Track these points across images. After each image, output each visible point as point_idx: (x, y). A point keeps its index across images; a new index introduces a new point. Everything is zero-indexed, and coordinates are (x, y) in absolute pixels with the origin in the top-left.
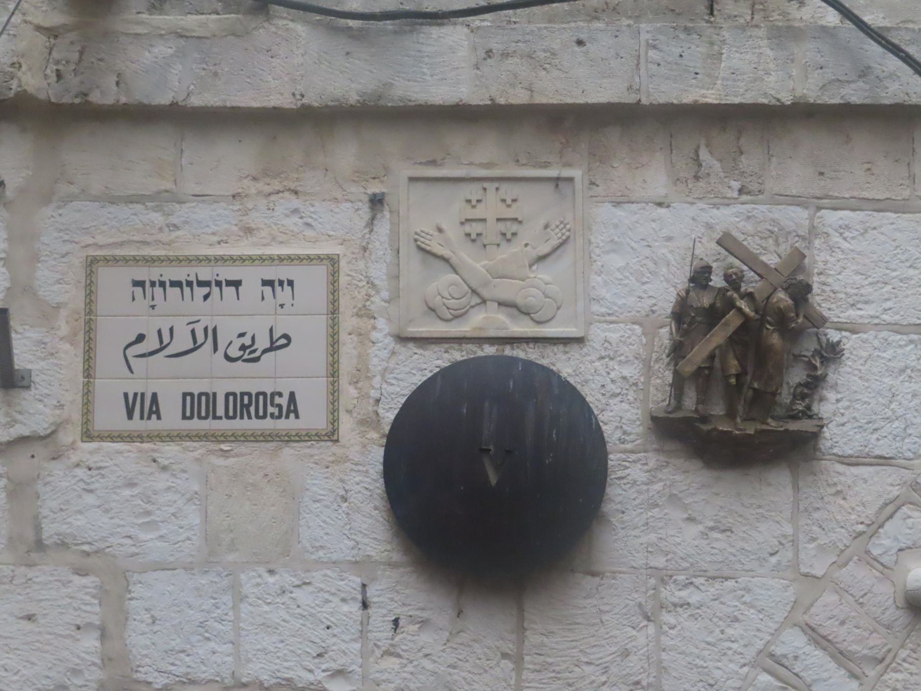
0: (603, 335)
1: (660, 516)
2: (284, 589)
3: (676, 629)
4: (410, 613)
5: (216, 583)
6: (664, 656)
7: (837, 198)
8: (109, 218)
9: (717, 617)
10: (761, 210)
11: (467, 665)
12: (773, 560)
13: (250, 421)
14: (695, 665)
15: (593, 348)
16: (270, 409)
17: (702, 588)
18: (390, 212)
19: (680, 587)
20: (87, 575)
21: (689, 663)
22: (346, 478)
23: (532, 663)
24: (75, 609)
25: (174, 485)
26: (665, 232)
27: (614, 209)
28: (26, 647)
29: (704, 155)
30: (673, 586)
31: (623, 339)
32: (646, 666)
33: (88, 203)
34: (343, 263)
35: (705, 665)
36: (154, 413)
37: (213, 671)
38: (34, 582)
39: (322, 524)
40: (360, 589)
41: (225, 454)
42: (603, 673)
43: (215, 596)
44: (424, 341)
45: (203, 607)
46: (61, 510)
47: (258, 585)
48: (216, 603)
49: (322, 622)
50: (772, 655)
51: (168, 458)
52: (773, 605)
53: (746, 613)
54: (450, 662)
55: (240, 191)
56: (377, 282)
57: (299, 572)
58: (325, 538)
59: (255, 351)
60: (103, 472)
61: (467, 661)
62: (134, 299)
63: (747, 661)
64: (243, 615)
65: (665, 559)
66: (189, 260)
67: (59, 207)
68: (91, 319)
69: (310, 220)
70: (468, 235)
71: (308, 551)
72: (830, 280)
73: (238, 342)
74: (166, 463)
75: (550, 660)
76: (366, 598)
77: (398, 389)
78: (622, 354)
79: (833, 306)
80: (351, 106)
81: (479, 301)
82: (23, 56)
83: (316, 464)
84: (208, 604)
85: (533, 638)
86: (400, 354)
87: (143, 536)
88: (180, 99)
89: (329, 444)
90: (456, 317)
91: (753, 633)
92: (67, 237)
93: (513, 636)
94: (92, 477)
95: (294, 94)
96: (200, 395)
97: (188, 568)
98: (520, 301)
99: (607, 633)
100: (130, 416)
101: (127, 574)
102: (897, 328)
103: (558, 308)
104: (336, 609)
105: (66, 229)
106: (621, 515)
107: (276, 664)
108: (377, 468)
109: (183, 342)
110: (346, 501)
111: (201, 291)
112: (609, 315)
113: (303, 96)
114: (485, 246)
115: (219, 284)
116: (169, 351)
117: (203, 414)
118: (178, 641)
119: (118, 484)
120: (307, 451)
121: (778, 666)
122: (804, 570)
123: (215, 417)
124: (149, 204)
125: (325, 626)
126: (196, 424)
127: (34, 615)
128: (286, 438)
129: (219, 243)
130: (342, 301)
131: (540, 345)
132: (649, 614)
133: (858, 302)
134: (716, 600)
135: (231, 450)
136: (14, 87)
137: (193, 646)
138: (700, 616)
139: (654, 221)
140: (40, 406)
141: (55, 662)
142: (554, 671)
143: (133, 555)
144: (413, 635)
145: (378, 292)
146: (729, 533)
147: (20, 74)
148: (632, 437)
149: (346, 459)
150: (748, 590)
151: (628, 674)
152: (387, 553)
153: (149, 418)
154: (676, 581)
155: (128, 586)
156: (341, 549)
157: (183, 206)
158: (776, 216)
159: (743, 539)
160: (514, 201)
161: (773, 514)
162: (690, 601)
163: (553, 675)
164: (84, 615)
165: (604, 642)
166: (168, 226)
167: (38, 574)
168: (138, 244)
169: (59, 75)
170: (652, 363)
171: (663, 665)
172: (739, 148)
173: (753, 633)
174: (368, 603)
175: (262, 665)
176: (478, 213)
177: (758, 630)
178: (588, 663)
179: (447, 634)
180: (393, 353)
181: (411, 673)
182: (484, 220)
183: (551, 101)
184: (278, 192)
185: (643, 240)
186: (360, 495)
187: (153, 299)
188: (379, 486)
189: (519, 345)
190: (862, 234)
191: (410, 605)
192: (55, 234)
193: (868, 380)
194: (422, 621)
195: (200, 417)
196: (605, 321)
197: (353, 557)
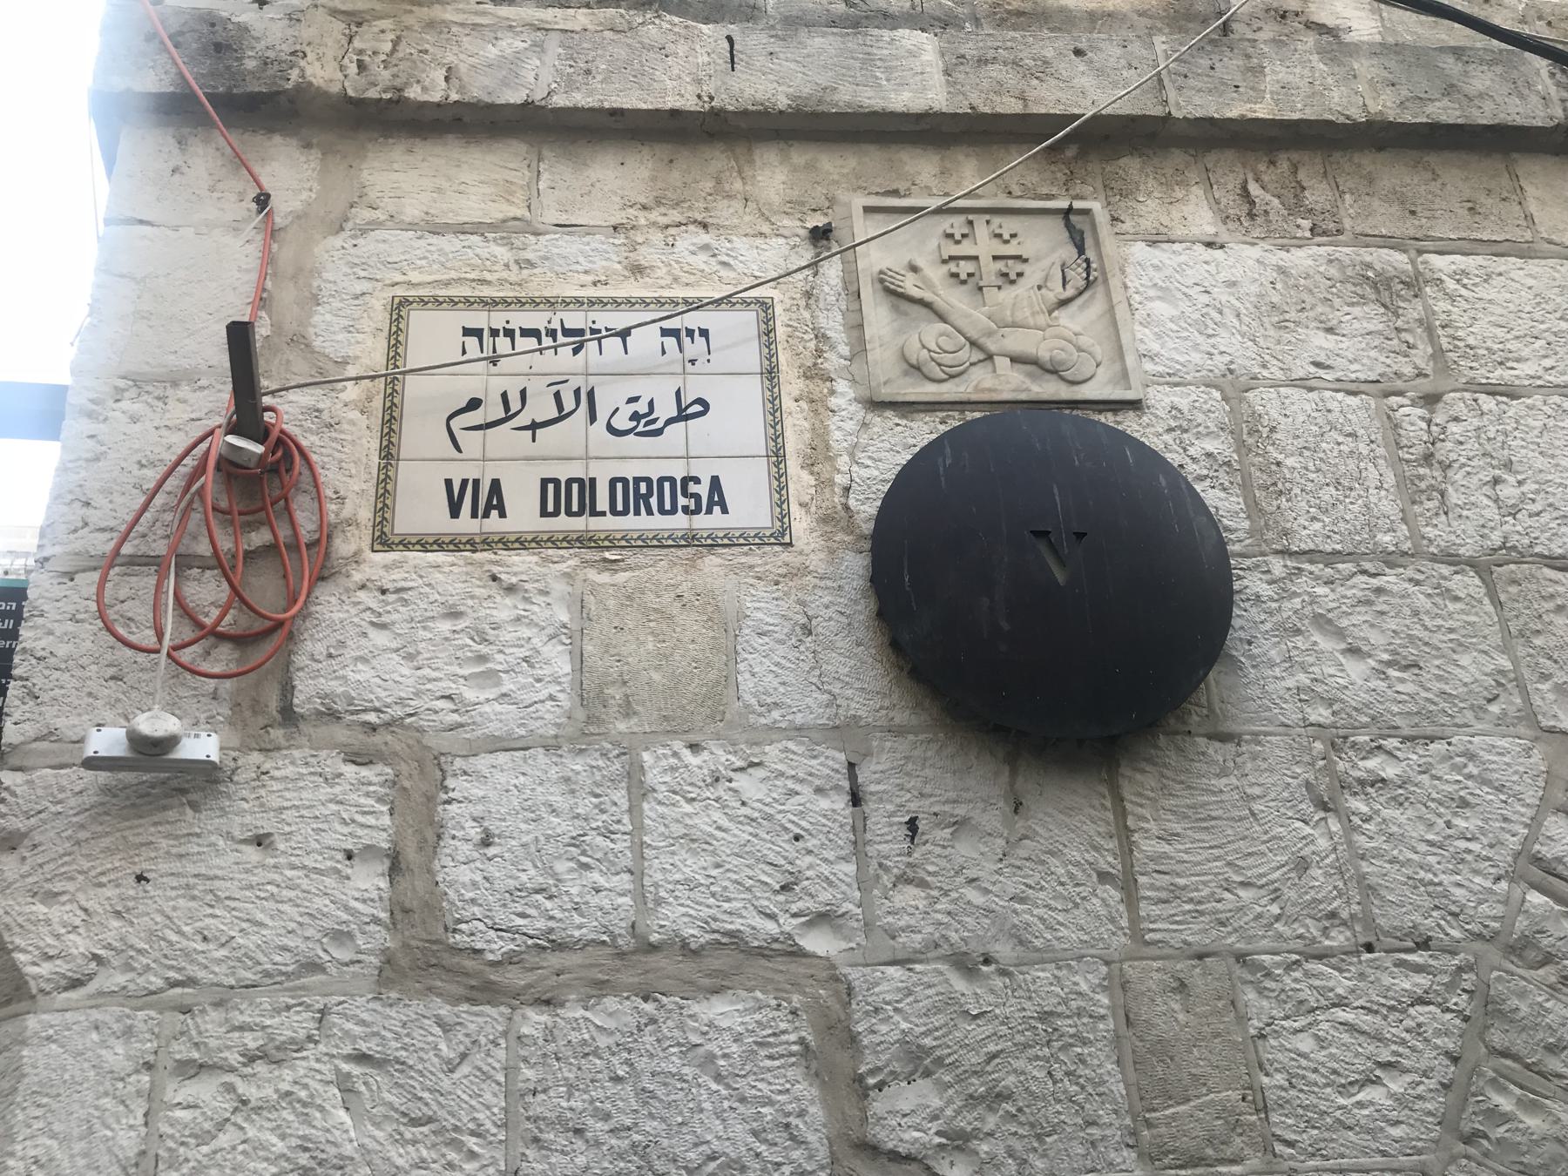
0: (1167, 400)
1: (1307, 646)
2: (717, 774)
3: (1372, 823)
4: (936, 809)
5: (599, 768)
6: (1365, 867)
7: (1441, 239)
8: (428, 251)
9: (1433, 800)
10: (1345, 252)
11: (1042, 895)
12: (1494, 709)
14: (1421, 881)
15: (1157, 417)
16: (682, 501)
17: (1398, 753)
19: (1364, 753)
20: (371, 762)
21: (1409, 878)
23: (1152, 887)
24: (344, 822)
25: (526, 614)
26: (1223, 276)
28: (248, 893)
29: (1254, 189)
30: (1351, 753)
31: (1197, 404)
32: (1340, 884)
34: (778, 310)
35: (1436, 880)
36: (495, 507)
37: (595, 924)
38: (272, 778)
39: (774, 669)
40: (845, 771)
42: (1273, 900)
44: (906, 408)
45: (579, 811)
46: (330, 656)
47: (673, 769)
48: (601, 803)
49: (786, 829)
50: (1537, 860)
51: (515, 574)
52: (1515, 778)
53: (1478, 792)
54: (1012, 891)
55: (625, 221)
56: (829, 334)
57: (743, 746)
58: (782, 689)
59: (654, 421)
60: (405, 596)
61: (1042, 889)
63: (1502, 872)
64: (647, 821)
65: (1330, 711)
66: (551, 303)
67: (354, 237)
69: (725, 259)
70: (955, 275)
71: (754, 712)
72: (1460, 333)
74: (514, 580)
75: (1181, 881)
77: (876, 473)
79: (1474, 364)
80: (781, 112)
81: (981, 356)
82: (309, 44)
83: (759, 578)
84: (585, 805)
85: (1147, 846)
86: (874, 425)
87: (470, 694)
88: (538, 96)
89: (777, 548)
90: (952, 377)
91: (1498, 825)
92: (363, 274)
93: (1112, 844)
94: (388, 604)
95: (699, 97)
96: (570, 482)
97: (551, 746)
98: (1044, 354)
99: (1266, 832)
100: (455, 511)
101: (443, 759)
103: (1097, 366)
104: (808, 805)
107: (709, 906)
108: (855, 583)
113: (712, 98)
114: (980, 289)
116: (516, 422)
117: (575, 508)
118: (532, 872)
119: (431, 614)
120: (743, 559)
121: (1551, 878)
122: (1545, 723)
123: (595, 513)
124: (490, 236)
125: (791, 835)
126: (563, 523)
127: (269, 835)
128: (709, 542)
129: (595, 284)
130: (783, 358)
132: (1326, 799)
133: (1508, 359)
134: (1424, 773)
135: (623, 560)
136: (294, 74)
137: (558, 880)
138: (1407, 799)
141: (300, 919)
142: (1191, 900)
144: (944, 847)
145: (833, 348)
146: (1417, 671)
147: (302, 63)
148: (1241, 535)
149: (803, 571)
150: (1472, 757)
151: (1314, 900)
152: (884, 712)
153: (486, 515)
154: (1354, 744)
155: (444, 779)
157: (541, 238)
158: (1368, 259)
159: (1439, 678)
160: (1013, 236)
161: (1474, 640)
162: (1384, 775)
163: (1187, 907)
164: (360, 832)
165: (1263, 848)
166: (517, 262)
168: (474, 284)
169: (361, 66)
170: (1245, 437)
171: (1367, 882)
172: (1298, 182)
173: (1498, 825)
175: (684, 910)
176: (966, 248)
177: (1506, 819)
178: (1243, 884)
179: (1001, 842)
180: (865, 425)
181: (949, 913)
182: (976, 258)
183: (1052, 111)
184: (679, 225)
188: (864, 610)
190: (1485, 281)
191: (931, 796)
192: (349, 271)
193: (1553, 456)
194: (955, 823)
195: (569, 513)
196: (1168, 383)
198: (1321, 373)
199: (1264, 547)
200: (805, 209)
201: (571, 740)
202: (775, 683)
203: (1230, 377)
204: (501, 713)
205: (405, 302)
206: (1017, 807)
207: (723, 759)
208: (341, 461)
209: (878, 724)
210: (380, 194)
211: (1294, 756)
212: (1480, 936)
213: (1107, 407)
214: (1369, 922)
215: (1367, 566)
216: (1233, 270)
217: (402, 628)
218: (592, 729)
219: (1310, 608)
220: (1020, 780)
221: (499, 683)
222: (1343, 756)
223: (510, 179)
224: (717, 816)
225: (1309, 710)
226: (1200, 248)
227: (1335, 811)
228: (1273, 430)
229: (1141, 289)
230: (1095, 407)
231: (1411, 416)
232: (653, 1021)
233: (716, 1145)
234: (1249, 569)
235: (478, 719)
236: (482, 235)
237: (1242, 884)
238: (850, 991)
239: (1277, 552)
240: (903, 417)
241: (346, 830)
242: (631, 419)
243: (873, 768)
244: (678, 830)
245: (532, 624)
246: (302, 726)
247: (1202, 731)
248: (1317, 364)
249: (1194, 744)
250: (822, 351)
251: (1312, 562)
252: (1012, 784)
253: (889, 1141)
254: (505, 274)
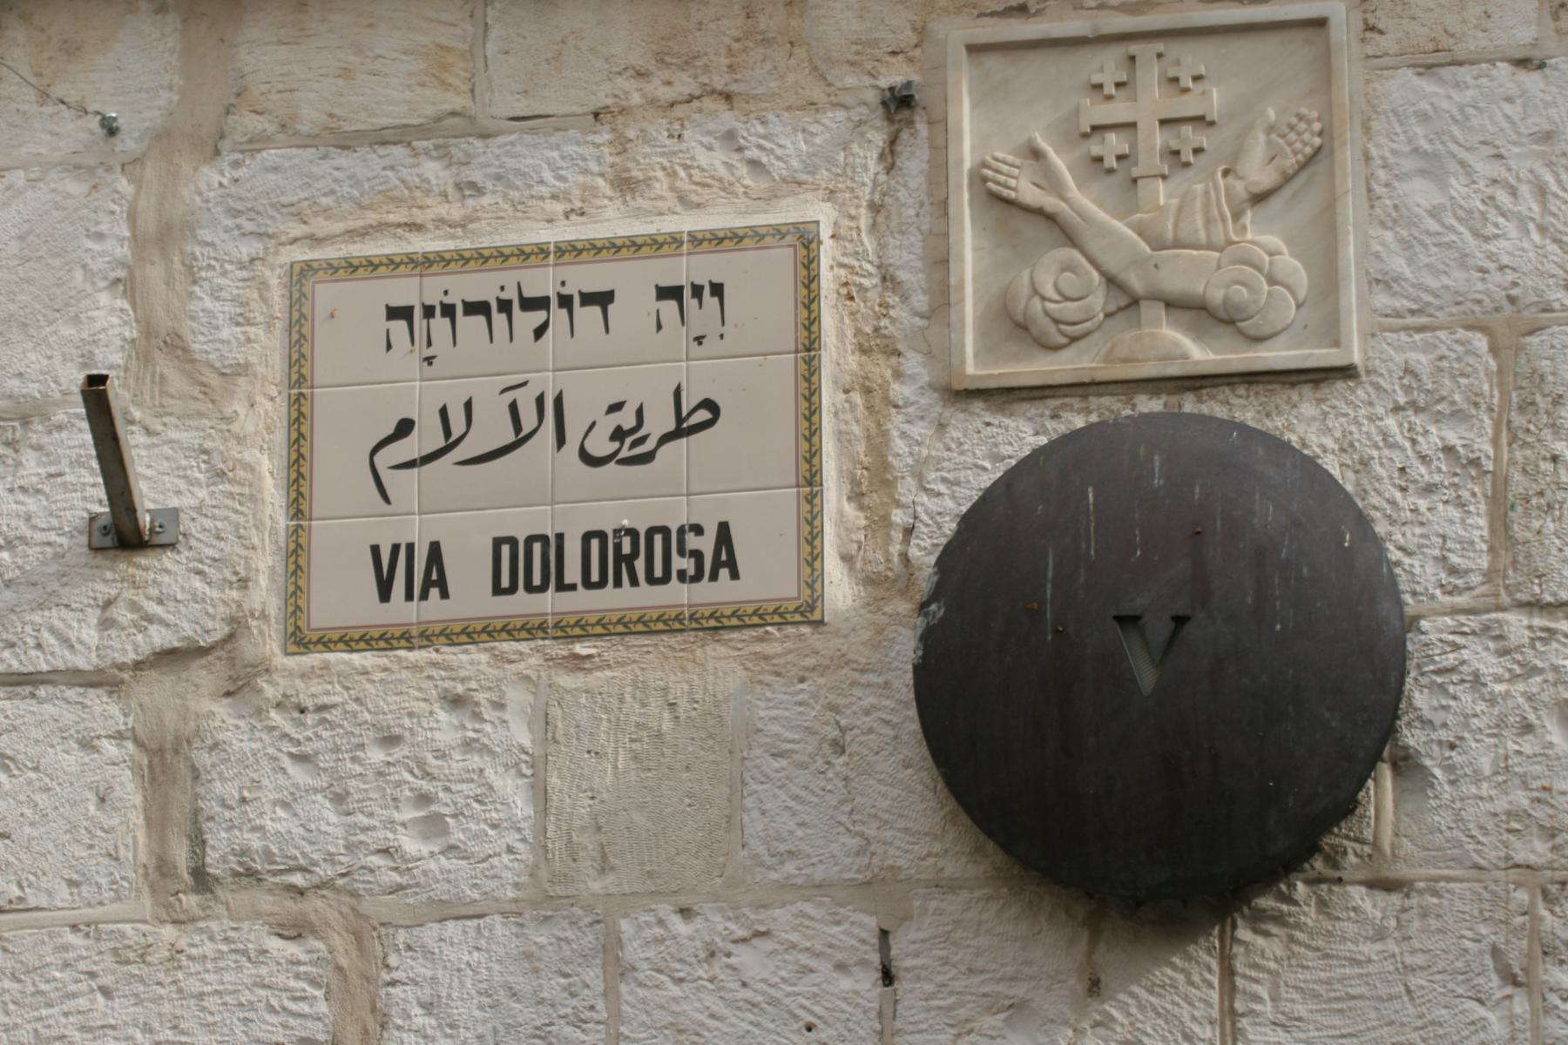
0: (1399, 358)
1: (1537, 750)
2: (713, 948)
4: (986, 989)
5: (567, 940)
8: (336, 181)
13: (635, 589)
15: (1378, 387)
16: (679, 563)
18: (930, 123)
20: (300, 935)
22: (841, 701)
24: (272, 1009)
26: (1538, 122)
27: (1416, 81)
33: (294, 151)
36: (434, 584)
38: (191, 958)
39: (792, 804)
40: (875, 941)
41: (577, 663)
43: (567, 970)
44: (1004, 396)
45: (545, 995)
47: (659, 941)
48: (570, 985)
49: (795, 1016)
55: (609, 101)
56: (902, 275)
58: (800, 833)
59: (642, 440)
60: (328, 716)
62: (389, 347)
64: (625, 1008)
65: (1549, 845)
67: (236, 164)
68: (301, 394)
71: (762, 864)
73: (608, 424)
74: (460, 689)
76: (890, 961)
78: (1443, 399)
81: (1123, 301)
83: (778, 674)
84: (553, 987)
89: (805, 630)
90: (1074, 339)
92: (249, 226)
96: (530, 540)
98: (1216, 296)
99: (1421, 1016)
100: (385, 593)
104: (824, 986)
105: (249, 210)
106: (1447, 754)
109: (492, 430)
110: (843, 752)
111: (527, 321)
112: (1412, 312)
114: (1135, 181)
115: (566, 301)
116: (461, 453)
117: (537, 581)
120: (758, 648)
123: (562, 587)
124: (420, 145)
125: (801, 1024)
126: (521, 603)
128: (712, 623)
131: (1260, 388)
132: (1517, 970)
139: (1509, 100)
140: (197, 583)
143: (398, 889)
145: (905, 298)
149: (843, 660)
152: (931, 860)
153: (424, 596)
156: (833, 856)
164: (292, 1022)
167: (197, 938)
168: (399, 230)
174: (894, 971)
176: (1118, 111)
182: (1132, 125)
184: (690, 99)
185: (1484, 143)
186: (872, 736)
187: (429, 344)
189: (1214, 391)
191: (982, 972)
192: (230, 223)
194: (1011, 1006)
195: (530, 588)
196: (1406, 328)
197: (858, 871)
199: (1505, 599)
200: (878, 53)
201: (534, 904)
202: (792, 824)
203: (1508, 310)
204: (449, 871)
205: (307, 268)
207: (721, 928)
208: (237, 526)
209: (923, 876)
210: (263, 88)
211: (1481, 912)
213: (1303, 378)
216: (1552, 111)
217: (325, 761)
218: (559, 890)
219: (1552, 690)
220: (1102, 947)
221: (445, 831)
222: (1557, 909)
223: (443, 41)
224: (710, 1000)
225: (1518, 845)
226: (1504, 68)
228: (1557, 401)
229: (1392, 160)
230: (1283, 378)
234: (1474, 633)
235: (422, 880)
236: (409, 144)
240: (1001, 410)
241: (274, 1019)
242: (613, 437)
243: (912, 936)
244: (663, 1017)
245: (485, 750)
246: (219, 891)
247: (1359, 876)
249: (1347, 897)
250: (887, 306)
252: (1089, 954)
254: (442, 210)
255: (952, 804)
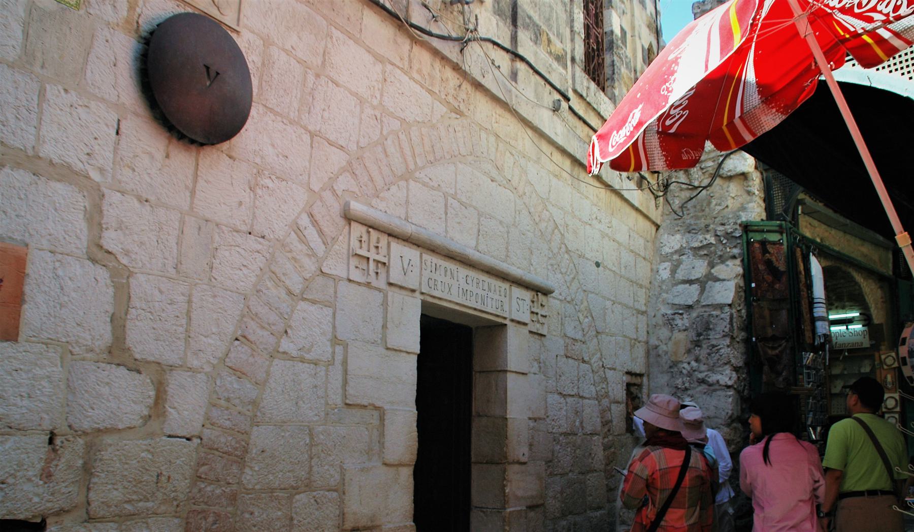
49: (92, 134)
61: (168, 184)
72: (331, 58)
102: (351, 93)
154: (264, 174)
198: (293, 51)
206: (167, 156)
212: (277, 240)
214: (252, 226)
215: (285, 121)
227: (253, 191)
231: (311, 78)
232: (37, 184)
233: (52, 231)
237: (224, 203)
238: (103, 195)
239: (263, 104)
247: (226, 152)
248: (292, 47)
251: (271, 112)
253: (106, 247)
255: (140, 93)
